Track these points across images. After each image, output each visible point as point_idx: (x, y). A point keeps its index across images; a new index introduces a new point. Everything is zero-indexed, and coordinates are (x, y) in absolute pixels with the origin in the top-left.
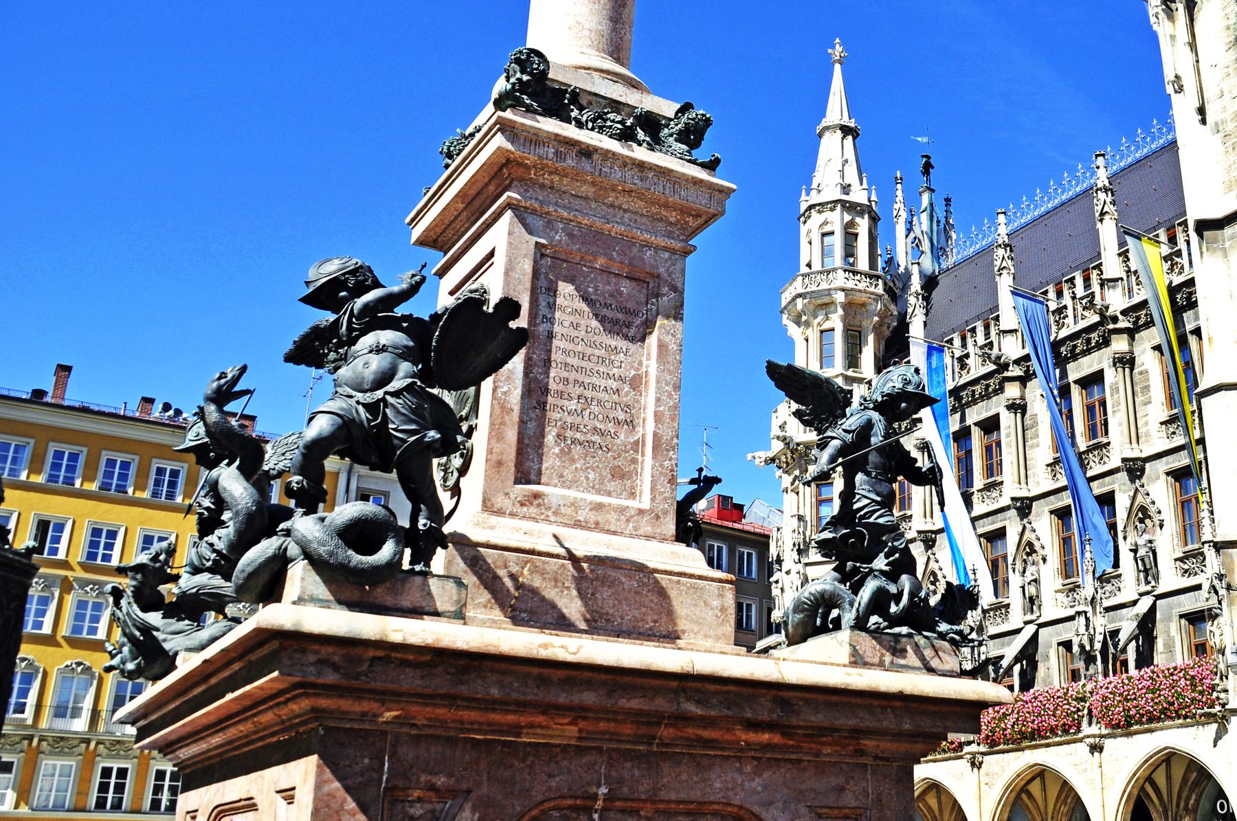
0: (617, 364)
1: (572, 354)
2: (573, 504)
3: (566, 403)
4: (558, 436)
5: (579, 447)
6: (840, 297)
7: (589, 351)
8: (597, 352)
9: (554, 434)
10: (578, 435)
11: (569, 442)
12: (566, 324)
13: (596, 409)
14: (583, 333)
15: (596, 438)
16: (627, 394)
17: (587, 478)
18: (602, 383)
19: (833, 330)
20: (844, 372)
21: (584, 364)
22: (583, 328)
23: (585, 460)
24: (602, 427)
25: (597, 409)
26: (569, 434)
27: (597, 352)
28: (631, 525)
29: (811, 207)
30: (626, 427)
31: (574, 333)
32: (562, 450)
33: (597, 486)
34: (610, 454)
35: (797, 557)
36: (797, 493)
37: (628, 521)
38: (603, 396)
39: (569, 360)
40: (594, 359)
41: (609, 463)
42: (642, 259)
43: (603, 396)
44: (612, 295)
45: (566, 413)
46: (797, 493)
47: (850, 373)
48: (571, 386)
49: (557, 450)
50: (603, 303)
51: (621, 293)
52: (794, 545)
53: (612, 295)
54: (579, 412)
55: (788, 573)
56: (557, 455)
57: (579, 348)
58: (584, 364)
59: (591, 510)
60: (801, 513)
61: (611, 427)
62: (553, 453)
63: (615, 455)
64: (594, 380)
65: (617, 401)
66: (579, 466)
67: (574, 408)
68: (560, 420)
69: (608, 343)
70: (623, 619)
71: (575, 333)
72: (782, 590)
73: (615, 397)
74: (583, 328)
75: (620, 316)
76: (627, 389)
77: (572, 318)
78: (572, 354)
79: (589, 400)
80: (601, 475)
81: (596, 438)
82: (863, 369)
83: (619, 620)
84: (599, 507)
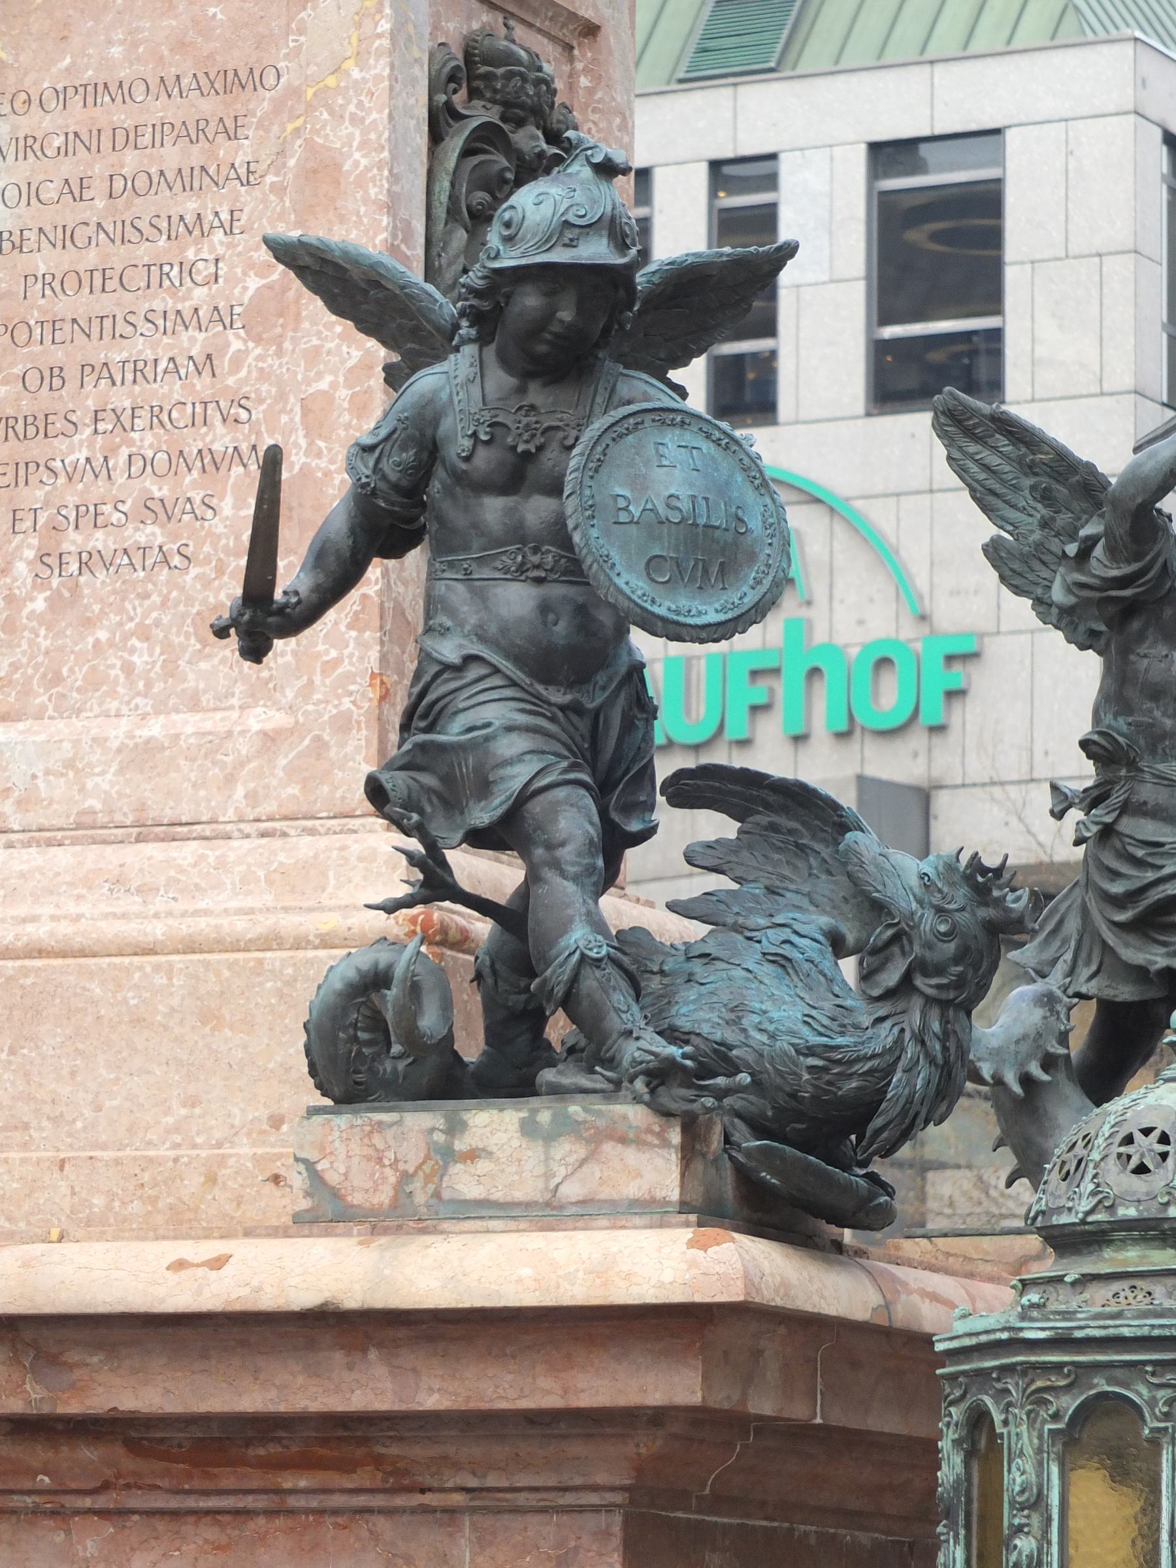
0: (204, 270)
1: (71, 283)
2: (70, 764)
3: (61, 444)
4: (41, 558)
5: (101, 575)
7: (119, 256)
8: (143, 253)
9: (30, 554)
10: (99, 540)
11: (74, 567)
12: (50, 192)
13: (145, 440)
14: (100, 204)
15: (152, 534)
16: (237, 362)
17: (128, 669)
18: (163, 349)
21: (105, 304)
22: (99, 188)
23: (121, 610)
24: (165, 492)
25: (149, 438)
26: (72, 541)
27: (143, 253)
28: (240, 792)
30: (238, 470)
31: (71, 213)
32: (56, 603)
33: (158, 687)
34: (194, 571)
37: (230, 780)
38: (169, 390)
39: (64, 306)
40: (137, 279)
41: (190, 601)
43: (169, 390)
44: (180, 46)
45: (62, 479)
48: (72, 385)
49: (39, 604)
50: (154, 83)
53: (180, 46)
54: (98, 461)
56: (40, 618)
57: (91, 258)
58: (105, 304)
59: (121, 771)
61: (191, 484)
62: (32, 615)
63: (209, 571)
64: (140, 348)
65: (207, 394)
66: (103, 635)
67: (82, 456)
68: (47, 503)
69: (175, 213)
70: (98, 1109)
71: (84, 212)
73: (202, 385)
74: (99, 188)
75: (209, 106)
76: (236, 345)
77: (68, 168)
78: (71, 283)
79: (126, 419)
80: (167, 647)
83: (88, 1113)
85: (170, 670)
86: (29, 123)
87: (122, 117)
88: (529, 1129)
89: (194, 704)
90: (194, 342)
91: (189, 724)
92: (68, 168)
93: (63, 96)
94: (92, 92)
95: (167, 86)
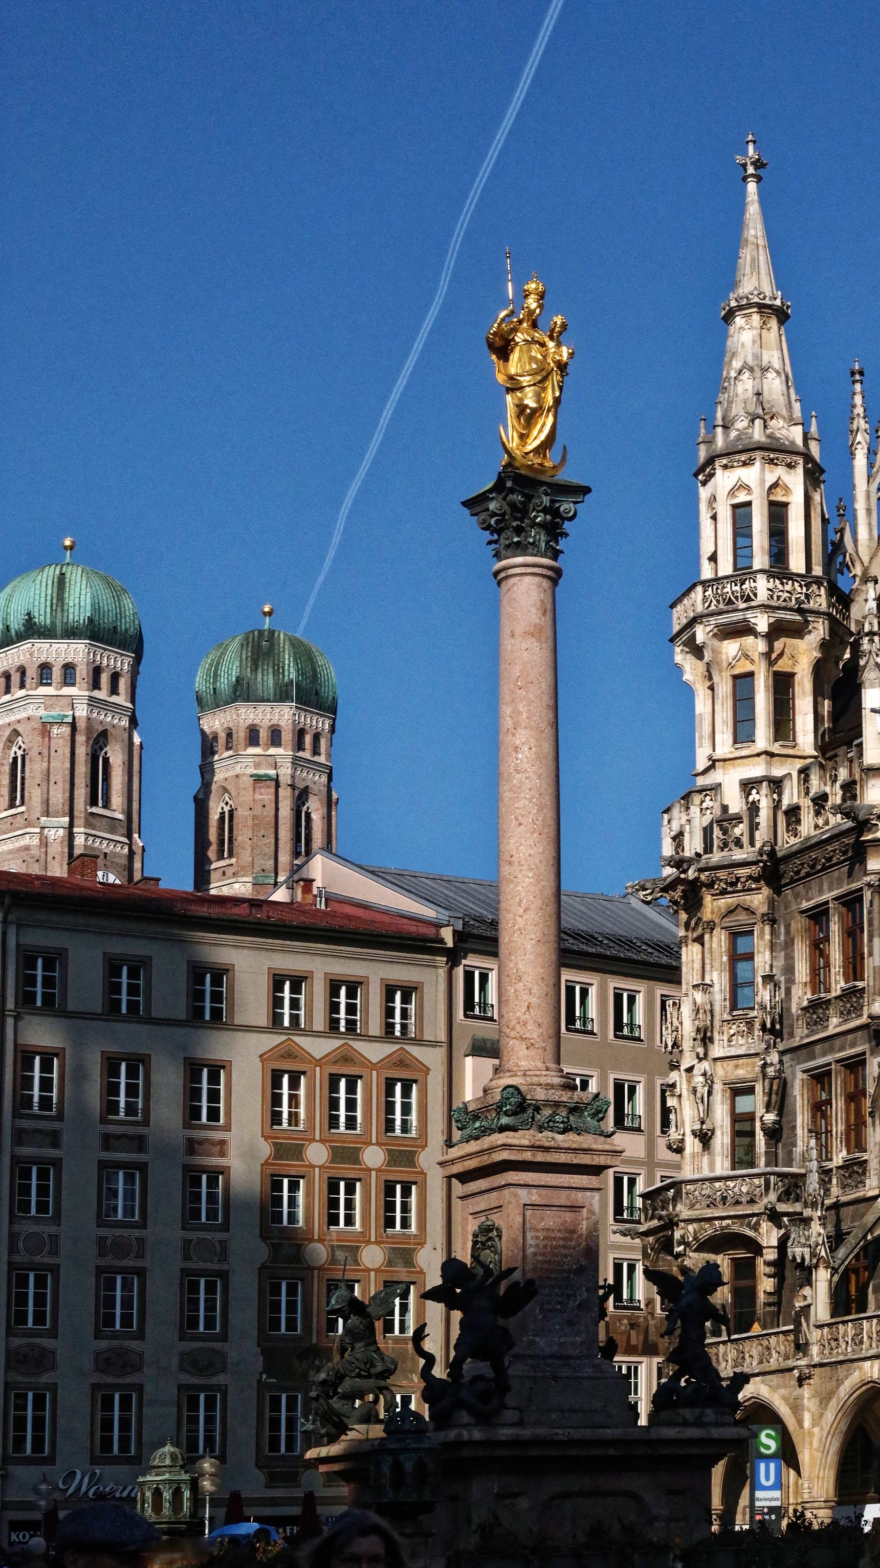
4: (540, 1310)
6: (762, 623)
10: (550, 1307)
15: (559, 1307)
19: (751, 675)
20: (769, 749)
29: (711, 461)
35: (701, 1050)
36: (703, 945)
42: (577, 1200)
46: (703, 945)
47: (776, 748)
49: (540, 1317)
51: (566, 1221)
52: (698, 1030)
55: (690, 1070)
60: (707, 981)
72: (680, 1096)
75: (567, 1235)
81: (559, 1307)
82: (800, 739)
84: (561, 1345)
85: (562, 1329)
86: (537, 1234)
87: (553, 1235)
88: (714, 1412)
89: (565, 1336)
90: (566, 1275)
91: (568, 1339)
92: (544, 1243)
93: (543, 1230)
94: (548, 1230)
95: (560, 1231)
